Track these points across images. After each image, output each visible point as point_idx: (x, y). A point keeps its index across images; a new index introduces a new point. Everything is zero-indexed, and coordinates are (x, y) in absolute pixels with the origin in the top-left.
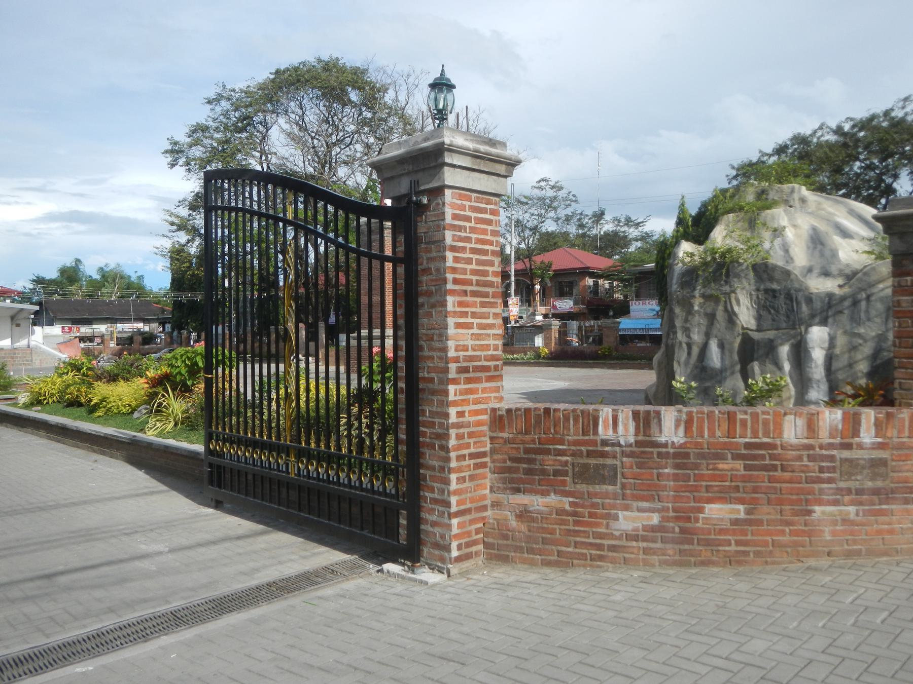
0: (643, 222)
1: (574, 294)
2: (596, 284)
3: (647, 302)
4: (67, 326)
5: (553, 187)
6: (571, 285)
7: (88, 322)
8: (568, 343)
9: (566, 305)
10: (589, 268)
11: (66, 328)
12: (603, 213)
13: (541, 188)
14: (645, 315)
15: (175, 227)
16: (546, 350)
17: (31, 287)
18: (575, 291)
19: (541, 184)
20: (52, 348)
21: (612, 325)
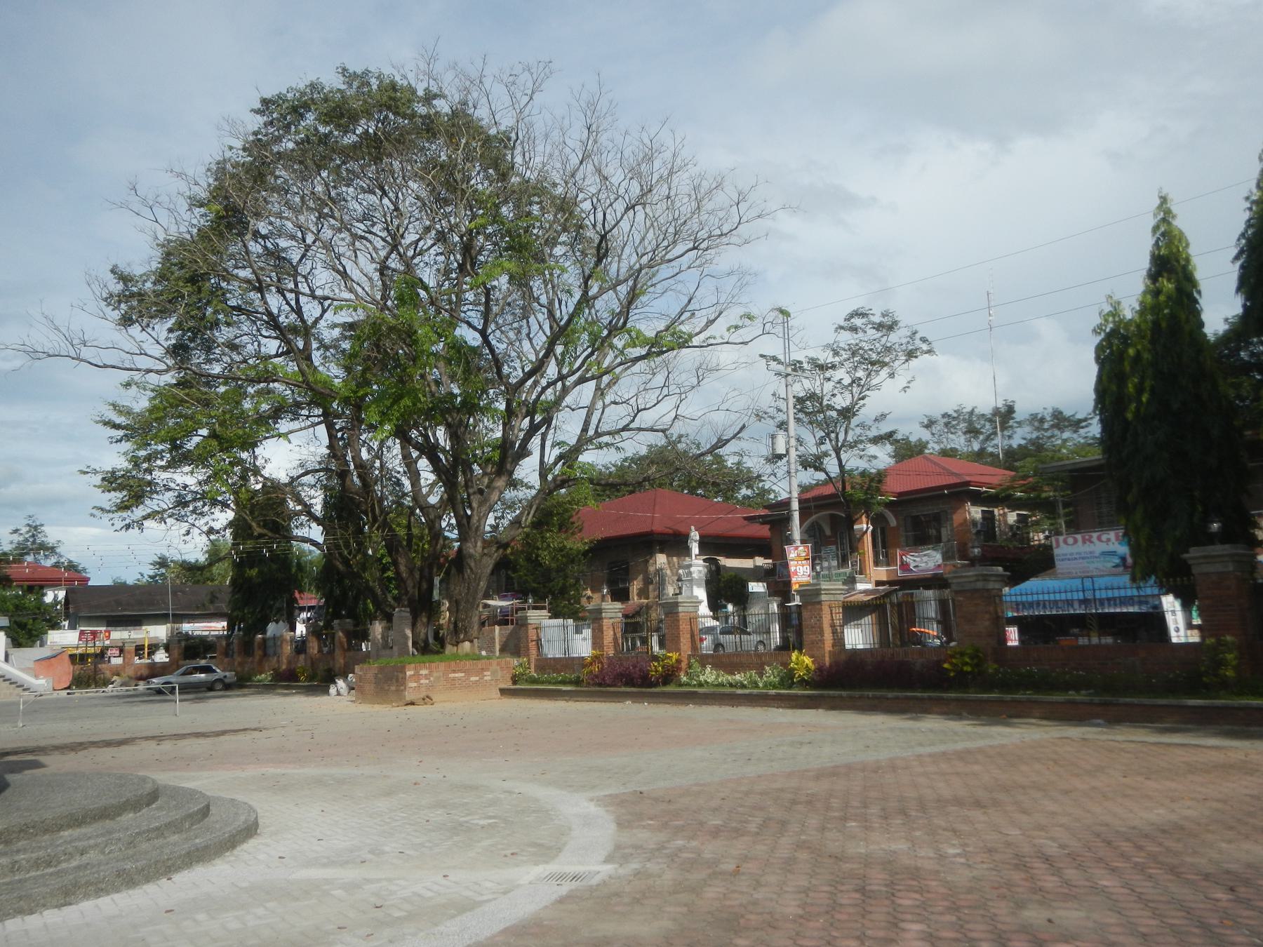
0: (1085, 420)
1: (944, 538)
2: (988, 518)
3: (1095, 535)
5: (879, 327)
6: (938, 520)
7: (135, 621)
8: (918, 639)
9: (926, 561)
10: (968, 483)
12: (1010, 410)
13: (854, 329)
14: (1092, 566)
15: (121, 433)
16: (807, 660)
17: (152, 573)
18: (945, 533)
19: (852, 320)
20: (23, 670)
21: (980, 585)
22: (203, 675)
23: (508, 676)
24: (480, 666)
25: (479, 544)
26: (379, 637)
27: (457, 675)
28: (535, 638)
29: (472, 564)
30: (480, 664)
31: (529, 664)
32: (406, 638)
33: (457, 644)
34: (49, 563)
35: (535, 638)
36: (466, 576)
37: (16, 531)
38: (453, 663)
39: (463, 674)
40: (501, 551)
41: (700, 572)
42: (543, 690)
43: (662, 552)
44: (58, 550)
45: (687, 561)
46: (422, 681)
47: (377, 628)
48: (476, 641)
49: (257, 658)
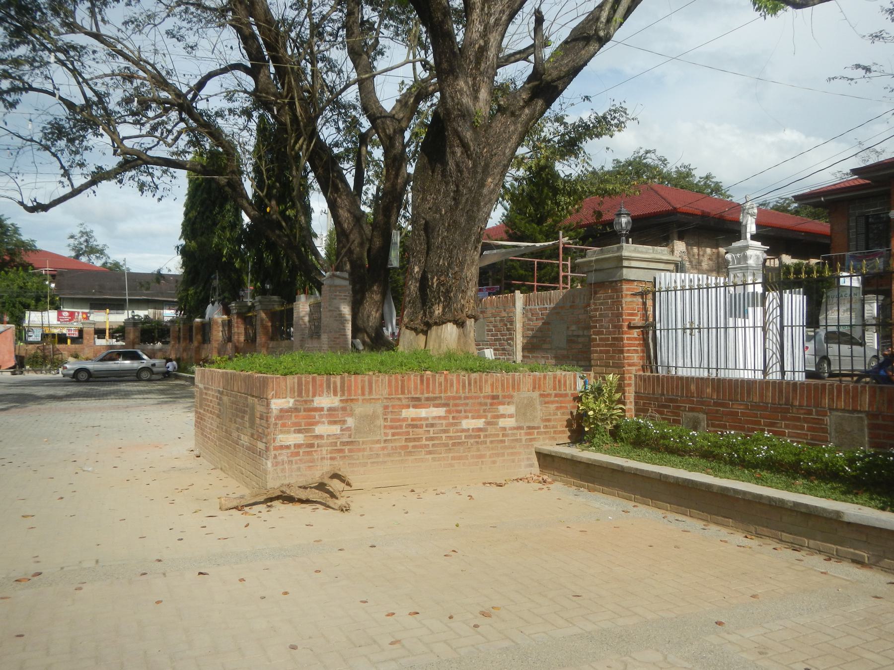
4: (66, 311)
11: (65, 314)
22: (128, 362)
23: (560, 420)
24: (487, 390)
25: (483, 94)
26: (307, 319)
27: (423, 413)
28: (638, 320)
29: (468, 135)
30: (489, 383)
31: (620, 388)
32: (341, 318)
33: (426, 328)
34: (98, 263)
35: (638, 320)
36: (451, 165)
37: (72, 237)
38: (413, 379)
39: (441, 412)
40: (540, 103)
41: (758, 258)
42: (724, 494)
43: (680, 238)
44: (105, 251)
45: (736, 244)
46: (320, 430)
47: (303, 306)
48: (470, 323)
49: (196, 343)
